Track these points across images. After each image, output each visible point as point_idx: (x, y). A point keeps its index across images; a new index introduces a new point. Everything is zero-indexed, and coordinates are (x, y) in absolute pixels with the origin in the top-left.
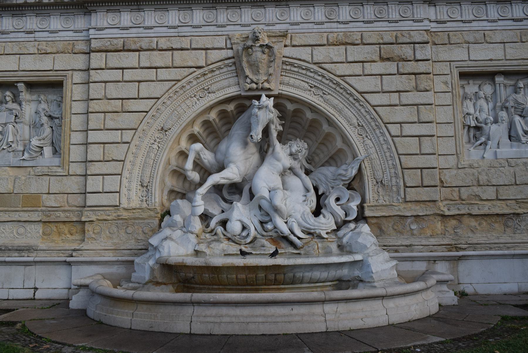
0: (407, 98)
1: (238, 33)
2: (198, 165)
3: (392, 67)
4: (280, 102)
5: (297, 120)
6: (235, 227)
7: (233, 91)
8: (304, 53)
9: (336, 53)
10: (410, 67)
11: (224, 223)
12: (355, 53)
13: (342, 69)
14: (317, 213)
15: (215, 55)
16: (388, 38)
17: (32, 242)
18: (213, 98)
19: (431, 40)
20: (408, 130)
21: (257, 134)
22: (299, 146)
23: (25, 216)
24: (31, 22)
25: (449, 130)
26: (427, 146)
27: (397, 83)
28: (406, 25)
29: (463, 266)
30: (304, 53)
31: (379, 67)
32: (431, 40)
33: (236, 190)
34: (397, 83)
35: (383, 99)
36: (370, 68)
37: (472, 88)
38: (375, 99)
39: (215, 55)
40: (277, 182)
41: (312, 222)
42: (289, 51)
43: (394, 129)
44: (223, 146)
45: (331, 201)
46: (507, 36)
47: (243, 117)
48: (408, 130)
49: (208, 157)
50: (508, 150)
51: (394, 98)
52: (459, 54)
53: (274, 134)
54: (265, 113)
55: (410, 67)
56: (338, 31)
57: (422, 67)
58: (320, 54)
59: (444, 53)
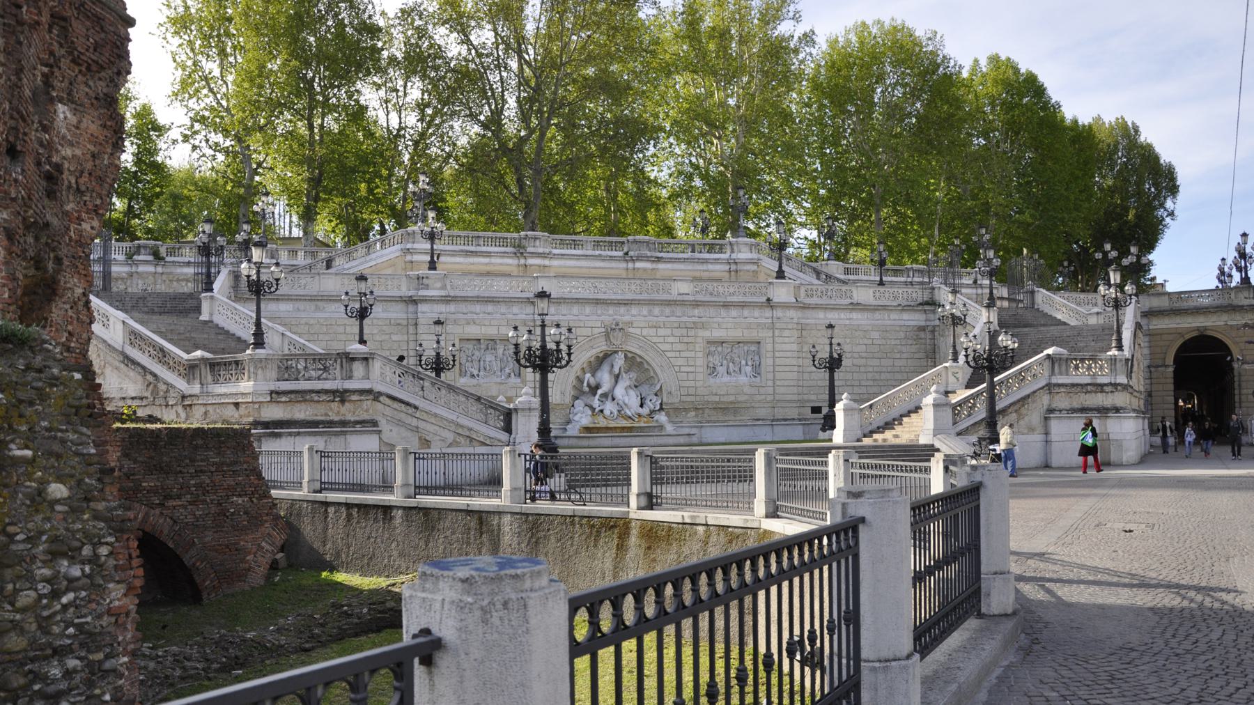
0: (683, 354)
1: (608, 320)
2: (589, 385)
4: (626, 352)
5: (634, 362)
6: (607, 412)
7: (604, 348)
8: (638, 331)
9: (652, 332)
10: (686, 340)
11: (602, 411)
12: (661, 332)
13: (655, 340)
14: (641, 406)
15: (596, 331)
16: (676, 325)
18: (594, 352)
19: (695, 326)
20: (683, 369)
21: (616, 370)
24: (503, 308)
25: (700, 369)
26: (691, 376)
27: (680, 347)
28: (685, 319)
29: (703, 430)
30: (638, 331)
31: (671, 339)
32: (695, 326)
33: (605, 395)
34: (680, 347)
35: (673, 354)
36: (668, 339)
37: (713, 349)
38: (669, 354)
39: (596, 331)
40: (623, 391)
41: (640, 410)
42: (631, 330)
43: (677, 369)
44: (599, 374)
45: (648, 401)
46: (729, 325)
47: (609, 360)
48: (683, 369)
49: (593, 382)
50: (726, 379)
52: (707, 334)
54: (619, 361)
55: (686, 340)
57: (690, 340)
58: (645, 332)
59: (701, 333)
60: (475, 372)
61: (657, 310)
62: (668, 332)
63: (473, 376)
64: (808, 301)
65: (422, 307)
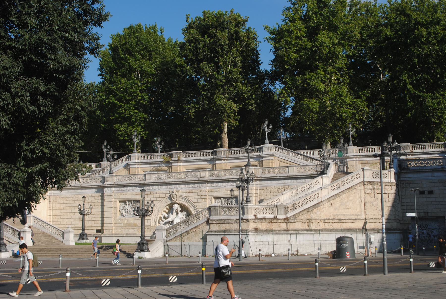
3: (200, 197)
12: (193, 194)
13: (190, 198)
17: (135, 233)
22: (184, 213)
23: (134, 228)
27: (200, 200)
31: (197, 197)
34: (200, 200)
36: (196, 197)
51: (200, 204)
53: (179, 211)
56: (190, 190)
57: (205, 197)
58: (186, 194)
60: (124, 214)
61: (191, 185)
62: (196, 194)
63: (123, 215)
64: (263, 176)
65: (106, 189)
